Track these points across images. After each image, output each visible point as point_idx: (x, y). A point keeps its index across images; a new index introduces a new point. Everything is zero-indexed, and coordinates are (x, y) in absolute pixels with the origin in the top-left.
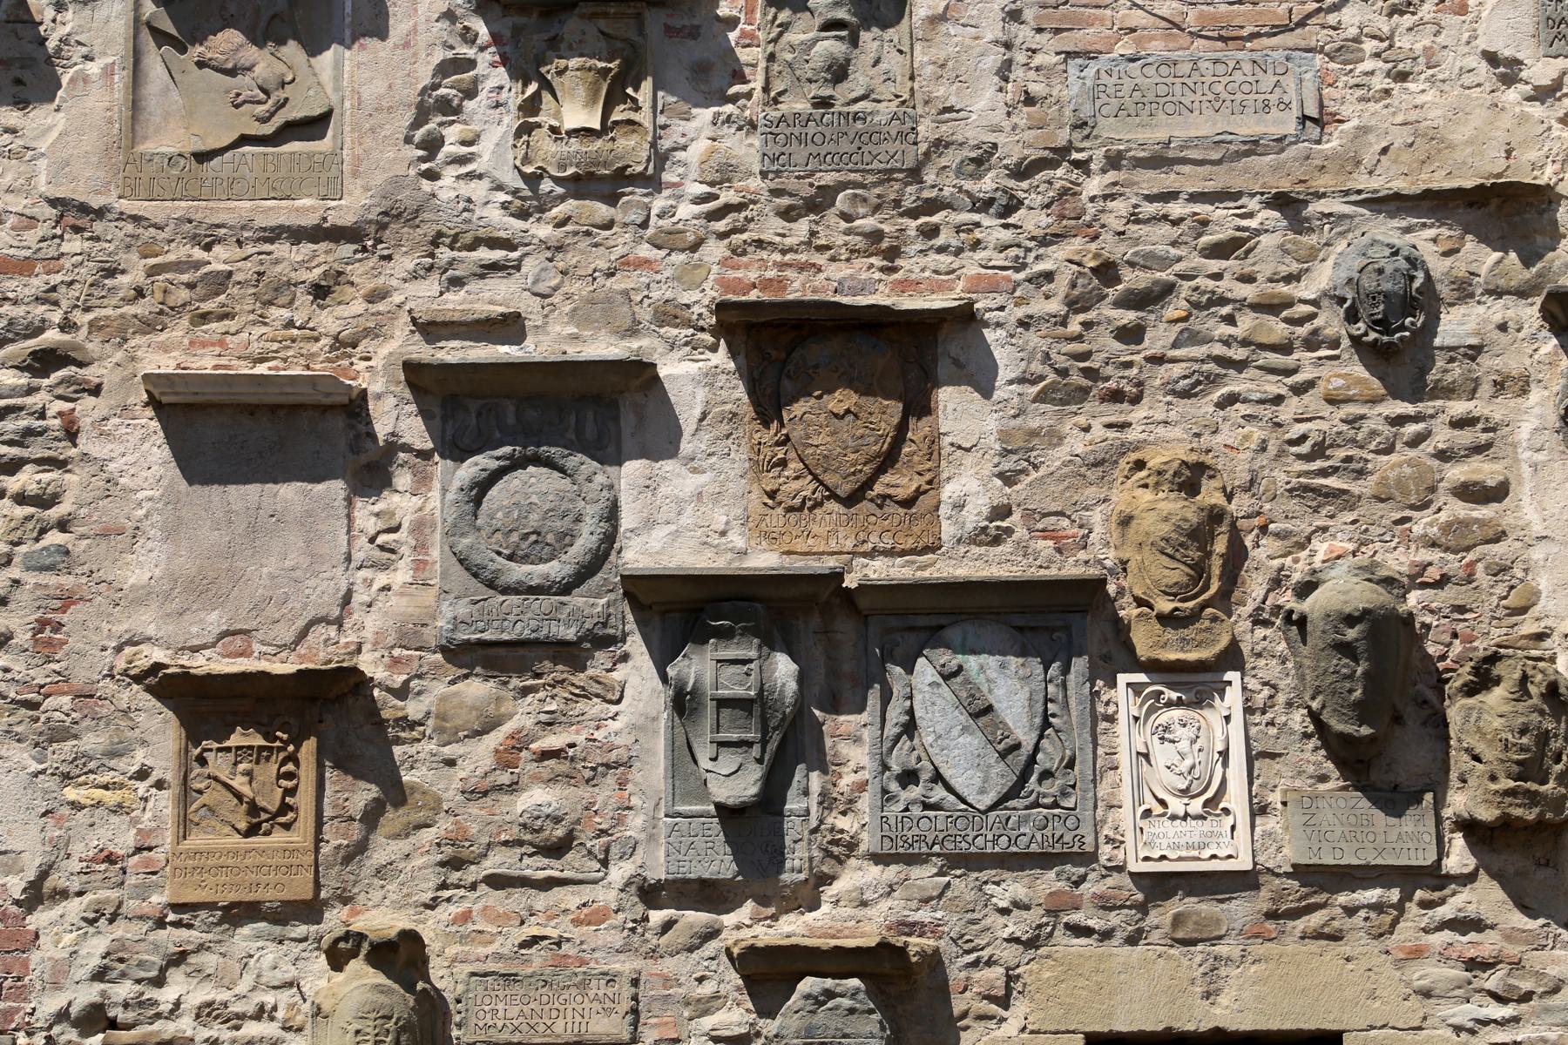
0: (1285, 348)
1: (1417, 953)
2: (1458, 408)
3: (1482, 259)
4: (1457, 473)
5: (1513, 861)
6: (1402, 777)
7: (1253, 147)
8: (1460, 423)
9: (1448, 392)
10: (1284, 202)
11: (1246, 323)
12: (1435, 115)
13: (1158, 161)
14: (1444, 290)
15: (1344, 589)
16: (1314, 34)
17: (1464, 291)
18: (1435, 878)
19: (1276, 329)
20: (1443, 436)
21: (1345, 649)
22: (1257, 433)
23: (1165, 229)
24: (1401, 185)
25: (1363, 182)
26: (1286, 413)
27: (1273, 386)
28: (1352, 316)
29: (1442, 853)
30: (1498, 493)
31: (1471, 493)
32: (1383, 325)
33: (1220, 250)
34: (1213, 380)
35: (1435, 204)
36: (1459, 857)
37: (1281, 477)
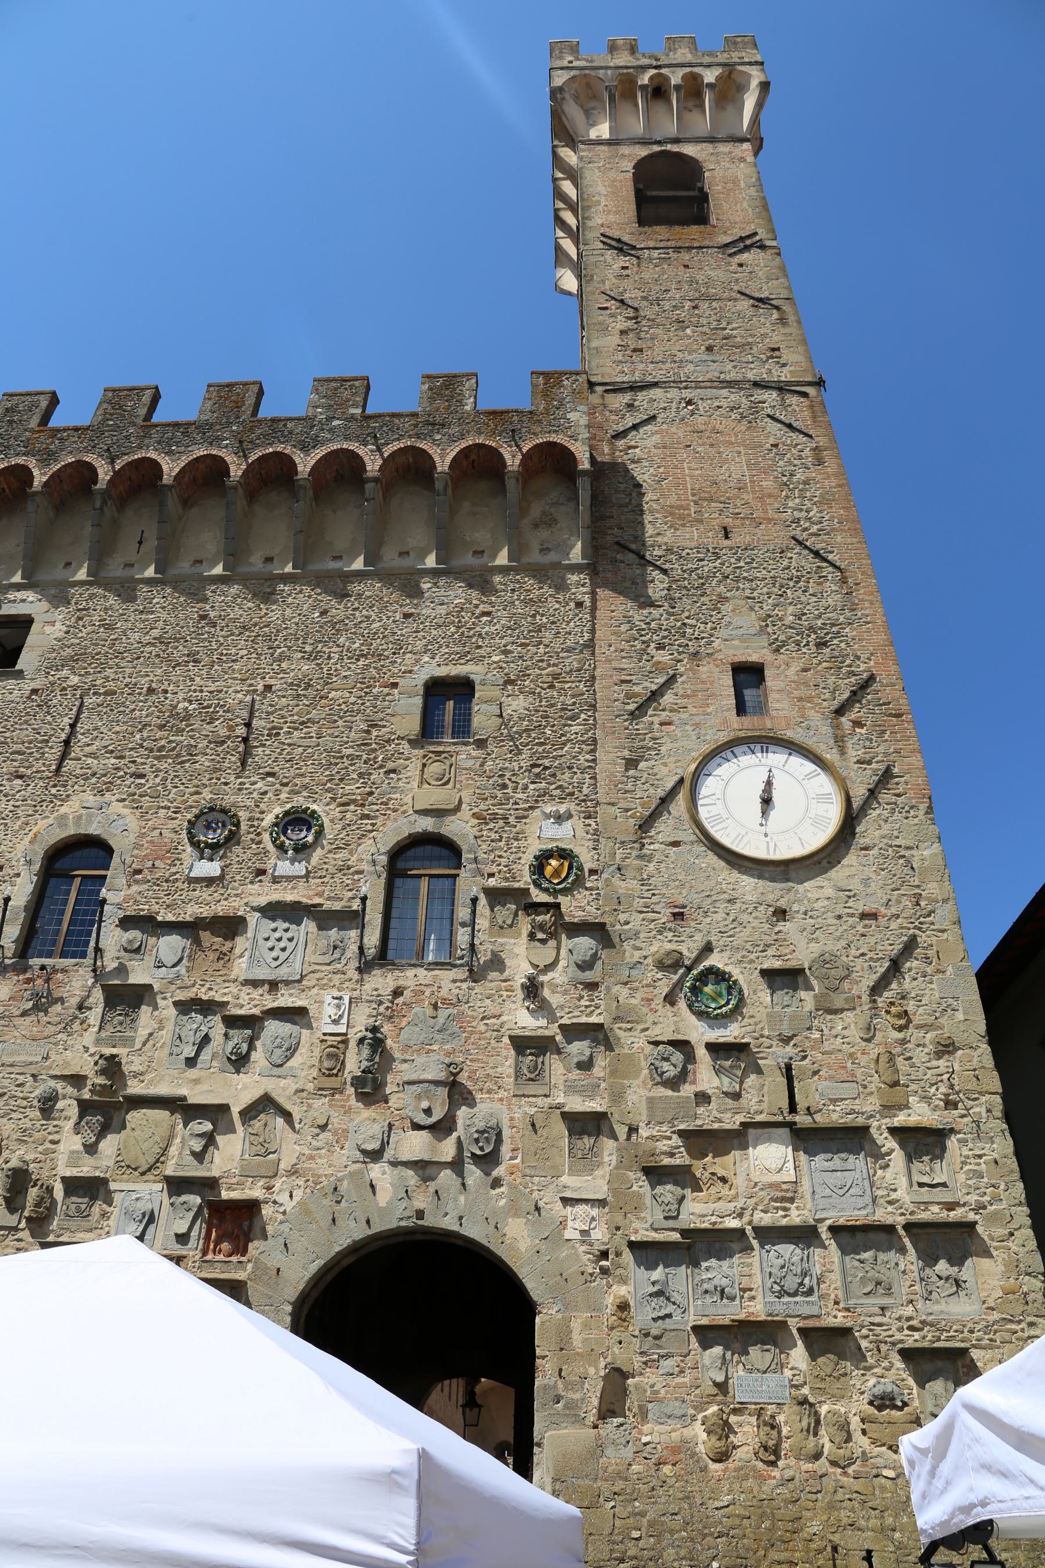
0: (25, 1108)
1: (7, 1246)
2: (55, 1123)
3: (70, 1090)
4: (51, 1137)
5: (33, 1226)
6: (17, 1206)
7: (31, 1063)
8: (55, 1126)
9: (55, 1119)
10: (34, 1076)
11: (19, 1101)
12: (69, 1059)
13: (11, 1065)
14: (60, 1097)
15: (14, 1163)
16: (52, 1040)
17: (64, 1097)
18: (16, 1229)
19: (25, 1103)
20: (51, 1129)
21: (7, 1176)
22: (13, 1126)
23: (9, 1080)
24: (59, 1073)
25: (53, 1072)
26: (20, 1122)
27: (21, 1116)
28: (39, 1101)
29: (19, 1222)
30: (57, 1142)
31: (53, 1142)
32: (43, 1104)
33: (18, 1086)
34: (9, 1114)
35: (63, 1077)
36: (23, 1225)
37: (15, 1137)
